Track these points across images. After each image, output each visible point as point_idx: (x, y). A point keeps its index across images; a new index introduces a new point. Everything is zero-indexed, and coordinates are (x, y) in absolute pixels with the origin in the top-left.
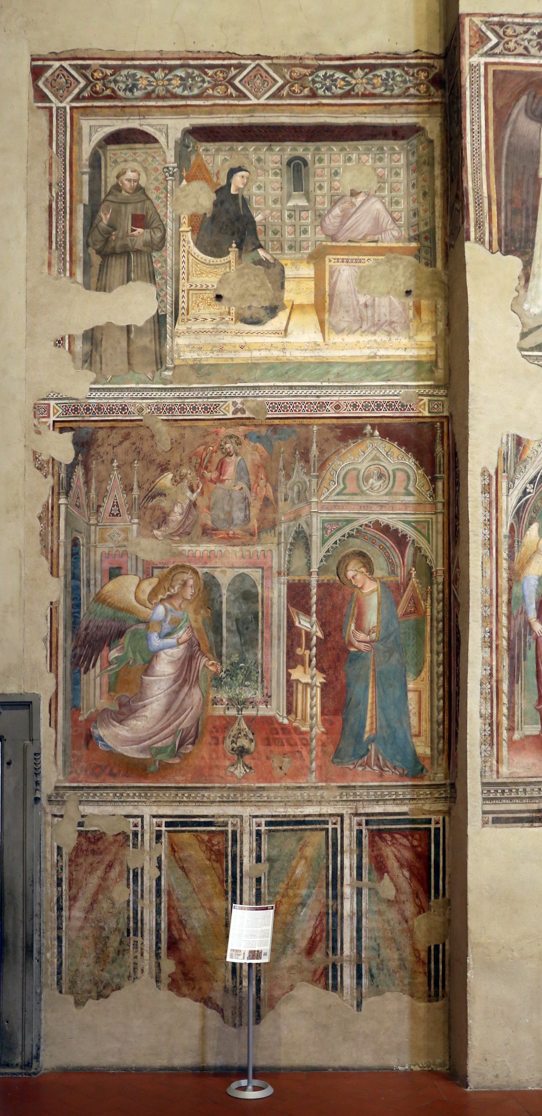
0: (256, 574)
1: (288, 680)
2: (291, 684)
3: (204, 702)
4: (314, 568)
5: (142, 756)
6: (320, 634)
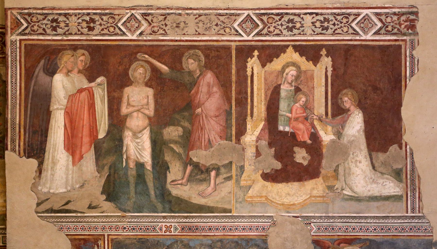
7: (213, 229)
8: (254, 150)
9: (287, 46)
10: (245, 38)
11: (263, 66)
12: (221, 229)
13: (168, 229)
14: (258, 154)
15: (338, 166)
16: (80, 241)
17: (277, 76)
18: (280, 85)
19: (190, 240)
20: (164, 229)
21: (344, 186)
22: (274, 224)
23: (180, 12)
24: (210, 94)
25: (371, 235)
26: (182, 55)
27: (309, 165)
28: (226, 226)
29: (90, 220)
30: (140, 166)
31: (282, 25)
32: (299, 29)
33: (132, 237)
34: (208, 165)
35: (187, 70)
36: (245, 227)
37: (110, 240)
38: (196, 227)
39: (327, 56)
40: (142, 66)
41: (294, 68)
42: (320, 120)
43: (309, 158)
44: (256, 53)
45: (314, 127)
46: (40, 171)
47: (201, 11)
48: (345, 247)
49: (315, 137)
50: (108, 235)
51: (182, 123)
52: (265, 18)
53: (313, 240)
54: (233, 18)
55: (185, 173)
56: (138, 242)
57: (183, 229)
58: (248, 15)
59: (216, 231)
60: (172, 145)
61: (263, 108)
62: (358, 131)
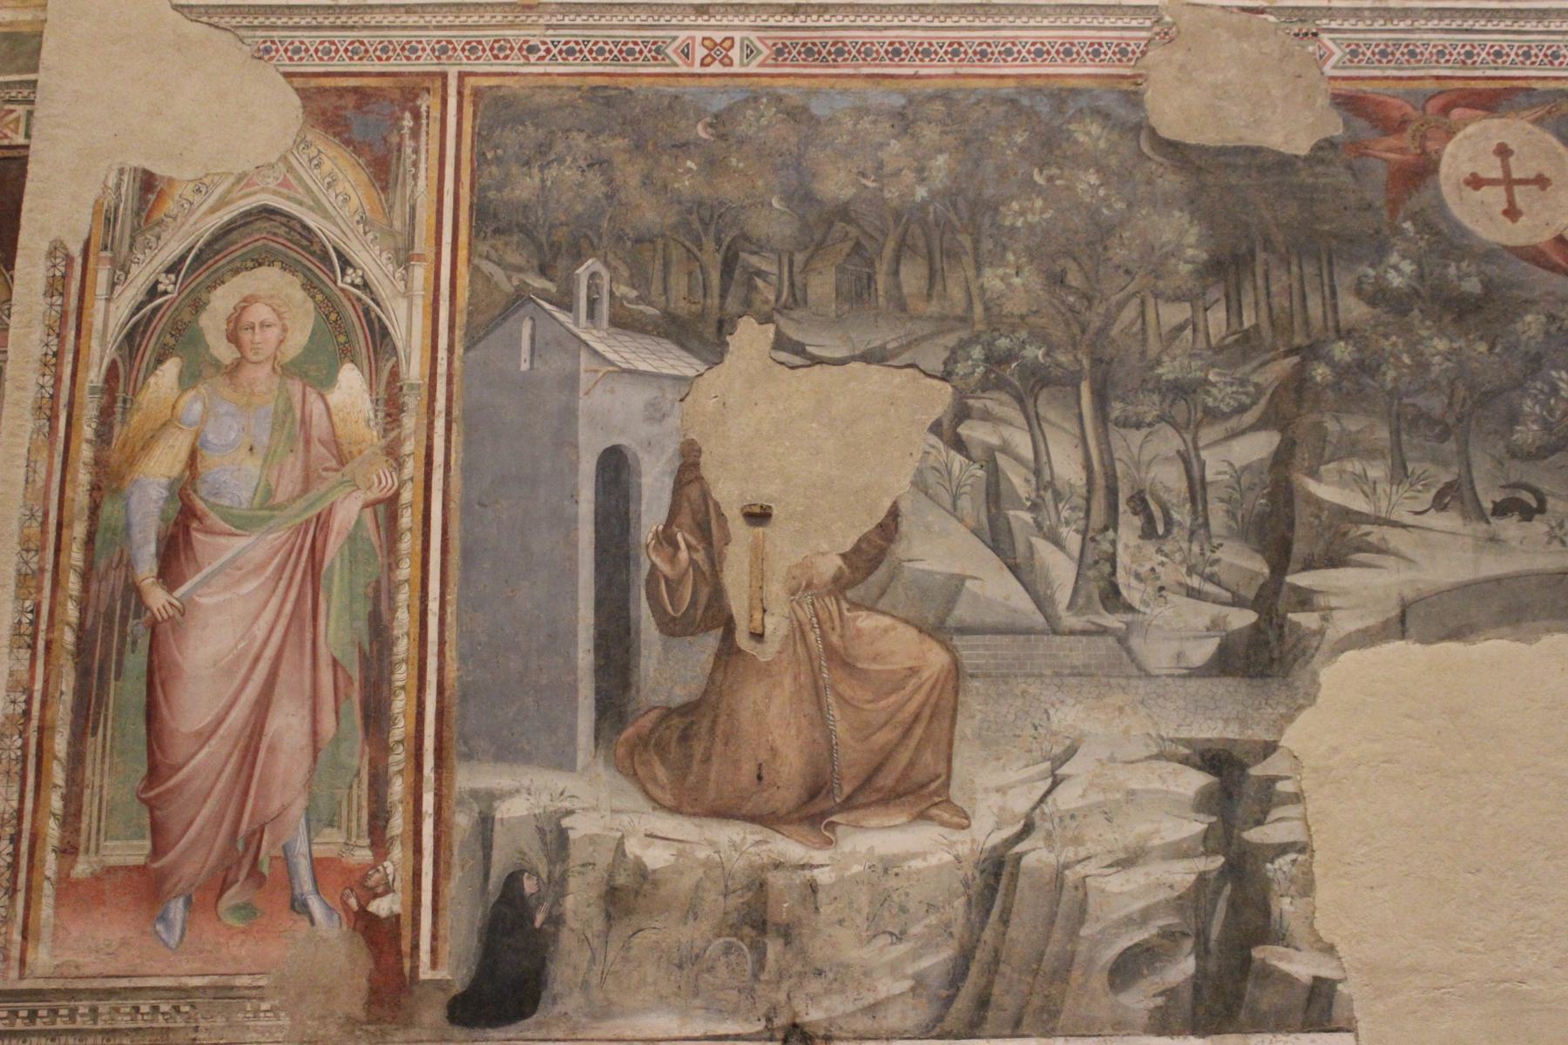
7: (907, 52)
12: (941, 52)
13: (717, 51)
16: (341, 97)
19: (816, 92)
20: (700, 52)
28: (963, 42)
29: (388, 19)
33: (562, 81)
36: (1043, 44)
37: (467, 92)
38: (834, 44)
48: (1473, 119)
53: (1335, 96)
56: (591, 100)
57: (779, 52)
59: (921, 60)
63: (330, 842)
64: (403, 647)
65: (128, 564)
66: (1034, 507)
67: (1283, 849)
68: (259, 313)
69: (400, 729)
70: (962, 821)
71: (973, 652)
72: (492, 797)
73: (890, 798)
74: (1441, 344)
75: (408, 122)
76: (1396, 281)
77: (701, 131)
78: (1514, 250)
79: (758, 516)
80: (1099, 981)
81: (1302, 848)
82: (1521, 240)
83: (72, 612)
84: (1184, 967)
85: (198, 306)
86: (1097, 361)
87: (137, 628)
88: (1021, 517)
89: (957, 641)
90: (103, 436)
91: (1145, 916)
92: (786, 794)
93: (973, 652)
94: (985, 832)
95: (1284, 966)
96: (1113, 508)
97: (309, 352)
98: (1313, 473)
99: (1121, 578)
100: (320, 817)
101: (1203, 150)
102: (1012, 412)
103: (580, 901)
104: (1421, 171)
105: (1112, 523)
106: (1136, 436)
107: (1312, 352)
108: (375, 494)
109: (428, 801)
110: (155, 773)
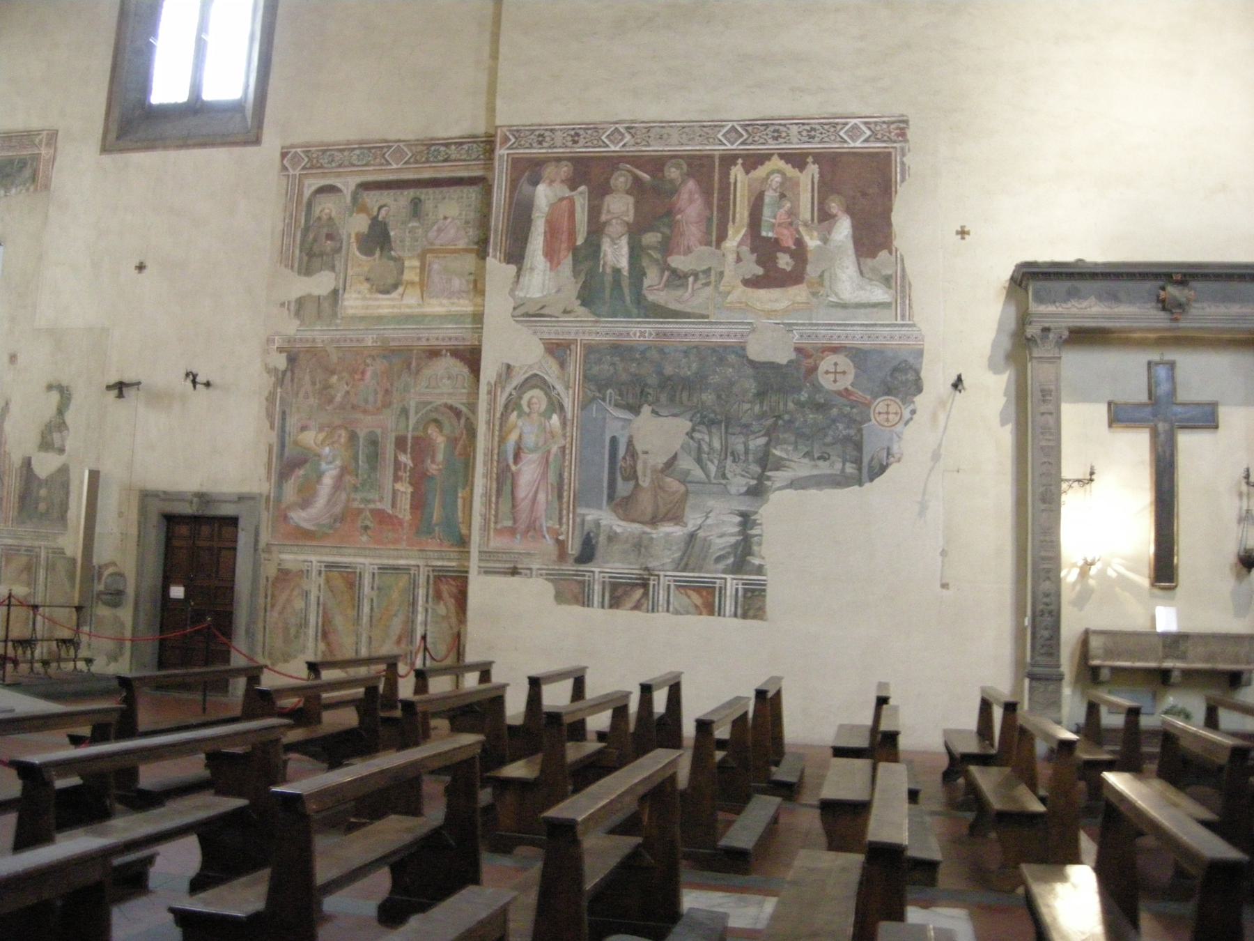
0: (379, 431)
1: (394, 490)
2: (395, 492)
3: (348, 500)
4: (410, 428)
5: (313, 528)
6: (412, 465)
8: (735, 256)
9: (772, 155)
10: (729, 147)
11: (747, 172)
13: (642, 334)
14: (739, 260)
15: (823, 272)
17: (762, 183)
18: (764, 192)
20: (638, 334)
21: (829, 292)
22: (753, 330)
23: (663, 125)
24: (691, 201)
25: (857, 343)
26: (663, 165)
27: (791, 271)
30: (617, 271)
31: (767, 135)
32: (784, 138)
34: (686, 270)
35: (668, 178)
39: (814, 163)
40: (624, 176)
41: (780, 175)
42: (806, 225)
43: (793, 263)
44: (740, 161)
45: (798, 232)
46: (518, 275)
47: (685, 124)
49: (799, 242)
50: (581, 340)
51: (662, 230)
52: (750, 129)
54: (718, 129)
55: (662, 279)
58: (733, 126)
60: (649, 251)
61: (746, 214)
62: (846, 236)
63: (550, 523)
64: (566, 481)
65: (506, 460)
66: (708, 454)
67: (757, 535)
68: (534, 400)
69: (565, 500)
70: (685, 525)
71: (691, 487)
72: (584, 515)
73: (670, 520)
74: (811, 416)
75: (568, 352)
76: (802, 399)
77: (637, 356)
78: (833, 391)
79: (646, 453)
80: (712, 562)
81: (760, 535)
82: (835, 389)
83: (495, 469)
84: (731, 560)
85: (520, 398)
86: (726, 418)
87: (509, 474)
88: (705, 456)
89: (688, 485)
90: (500, 430)
91: (724, 548)
92: (648, 517)
93: (691, 487)
94: (691, 527)
95: (753, 561)
96: (726, 455)
97: (546, 411)
98: (775, 448)
99: (726, 472)
100: (549, 518)
101: (759, 363)
102: (706, 431)
103: (602, 539)
104: (814, 369)
105: (726, 458)
106: (733, 437)
107: (779, 417)
108: (560, 445)
109: (571, 516)
110: (514, 506)
